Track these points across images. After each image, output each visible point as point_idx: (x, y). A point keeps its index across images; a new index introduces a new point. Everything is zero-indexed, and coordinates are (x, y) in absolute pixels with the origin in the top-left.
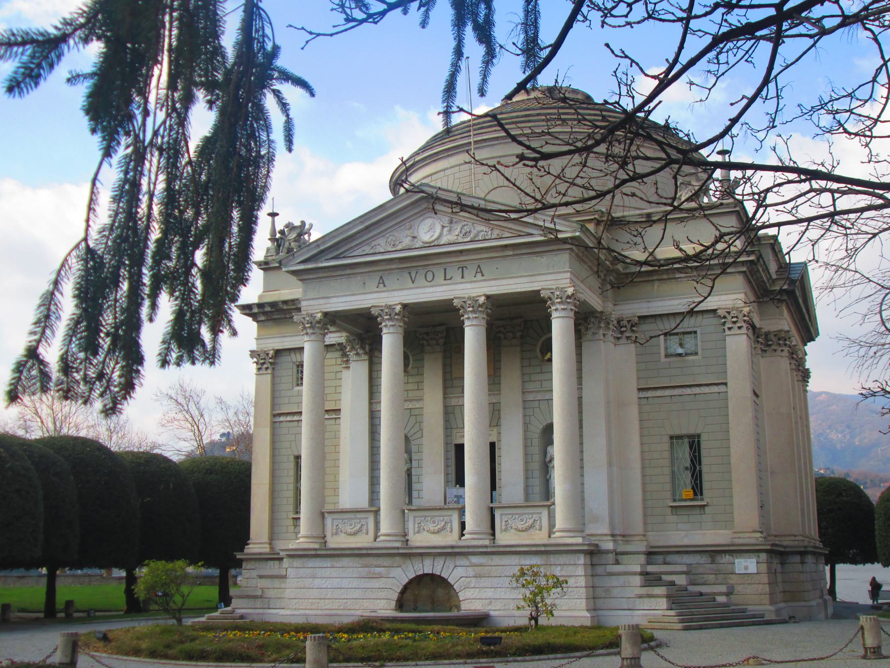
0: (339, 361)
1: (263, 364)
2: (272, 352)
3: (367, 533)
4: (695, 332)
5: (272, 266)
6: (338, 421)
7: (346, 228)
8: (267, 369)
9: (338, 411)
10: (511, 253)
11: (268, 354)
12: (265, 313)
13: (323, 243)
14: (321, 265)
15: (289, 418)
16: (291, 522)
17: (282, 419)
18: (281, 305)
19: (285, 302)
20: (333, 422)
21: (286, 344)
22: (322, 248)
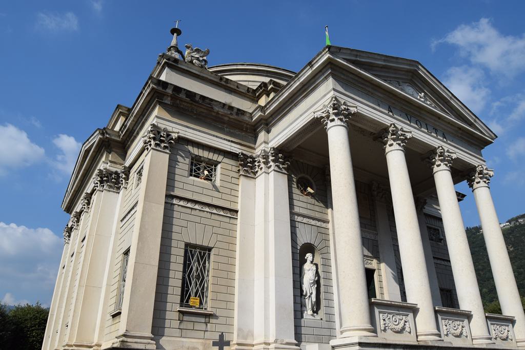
0: (236, 169)
1: (162, 141)
2: (174, 136)
3: (410, 333)
4: (438, 230)
5: (179, 66)
6: (232, 221)
7: (376, 57)
8: (165, 147)
9: (237, 212)
10: (459, 135)
11: (168, 135)
12: (173, 98)
13: (360, 56)
14: (359, 70)
15: (182, 203)
16: (176, 316)
17: (175, 201)
18: (197, 98)
19: (203, 98)
20: (227, 220)
21: (187, 133)
22: (358, 59)
